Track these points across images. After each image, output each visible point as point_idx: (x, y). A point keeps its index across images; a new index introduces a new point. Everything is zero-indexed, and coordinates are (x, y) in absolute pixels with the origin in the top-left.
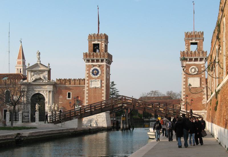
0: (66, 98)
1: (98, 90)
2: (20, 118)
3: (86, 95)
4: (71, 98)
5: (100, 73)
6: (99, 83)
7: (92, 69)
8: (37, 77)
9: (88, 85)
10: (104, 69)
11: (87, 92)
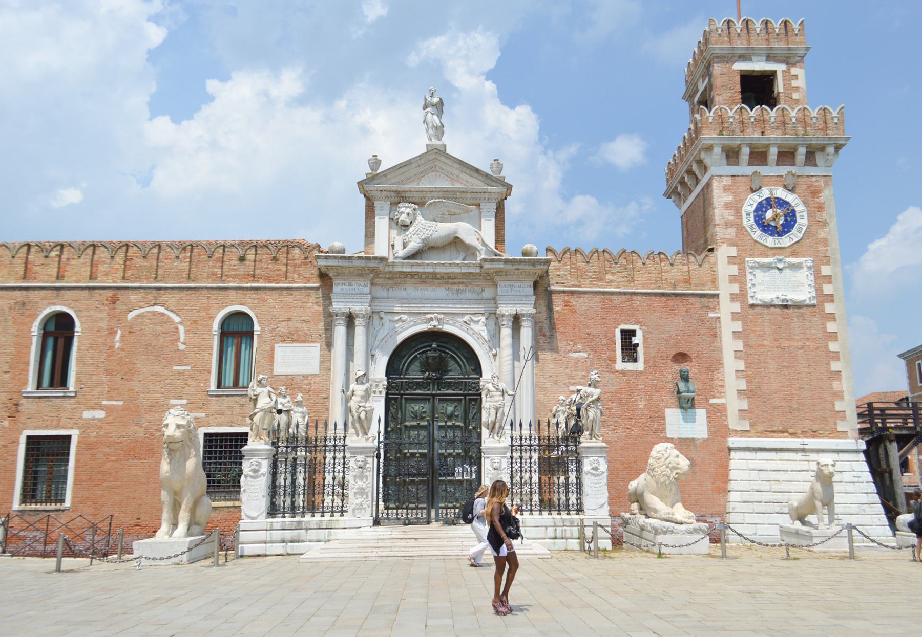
0: (614, 362)
1: (802, 315)
2: (361, 492)
3: (729, 346)
4: (640, 366)
5: (802, 221)
6: (805, 277)
7: (754, 200)
8: (427, 228)
9: (735, 288)
10: (822, 200)
11: (738, 326)
